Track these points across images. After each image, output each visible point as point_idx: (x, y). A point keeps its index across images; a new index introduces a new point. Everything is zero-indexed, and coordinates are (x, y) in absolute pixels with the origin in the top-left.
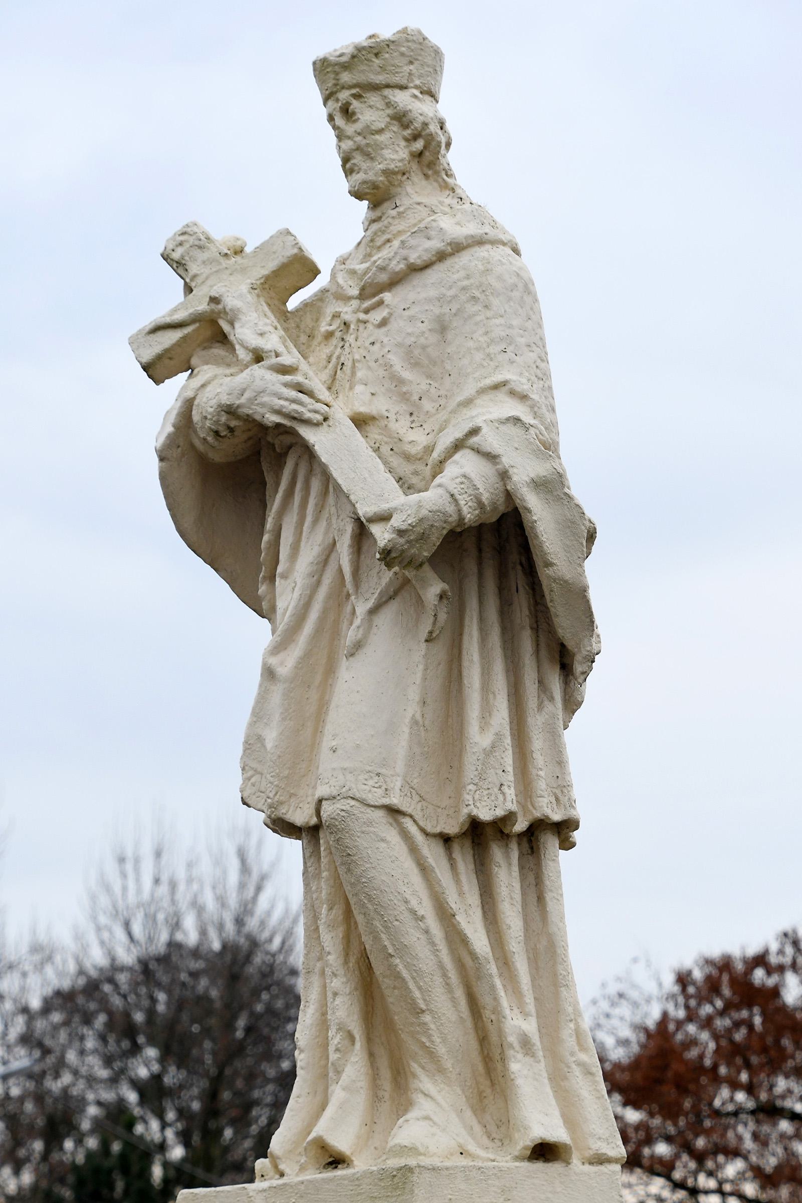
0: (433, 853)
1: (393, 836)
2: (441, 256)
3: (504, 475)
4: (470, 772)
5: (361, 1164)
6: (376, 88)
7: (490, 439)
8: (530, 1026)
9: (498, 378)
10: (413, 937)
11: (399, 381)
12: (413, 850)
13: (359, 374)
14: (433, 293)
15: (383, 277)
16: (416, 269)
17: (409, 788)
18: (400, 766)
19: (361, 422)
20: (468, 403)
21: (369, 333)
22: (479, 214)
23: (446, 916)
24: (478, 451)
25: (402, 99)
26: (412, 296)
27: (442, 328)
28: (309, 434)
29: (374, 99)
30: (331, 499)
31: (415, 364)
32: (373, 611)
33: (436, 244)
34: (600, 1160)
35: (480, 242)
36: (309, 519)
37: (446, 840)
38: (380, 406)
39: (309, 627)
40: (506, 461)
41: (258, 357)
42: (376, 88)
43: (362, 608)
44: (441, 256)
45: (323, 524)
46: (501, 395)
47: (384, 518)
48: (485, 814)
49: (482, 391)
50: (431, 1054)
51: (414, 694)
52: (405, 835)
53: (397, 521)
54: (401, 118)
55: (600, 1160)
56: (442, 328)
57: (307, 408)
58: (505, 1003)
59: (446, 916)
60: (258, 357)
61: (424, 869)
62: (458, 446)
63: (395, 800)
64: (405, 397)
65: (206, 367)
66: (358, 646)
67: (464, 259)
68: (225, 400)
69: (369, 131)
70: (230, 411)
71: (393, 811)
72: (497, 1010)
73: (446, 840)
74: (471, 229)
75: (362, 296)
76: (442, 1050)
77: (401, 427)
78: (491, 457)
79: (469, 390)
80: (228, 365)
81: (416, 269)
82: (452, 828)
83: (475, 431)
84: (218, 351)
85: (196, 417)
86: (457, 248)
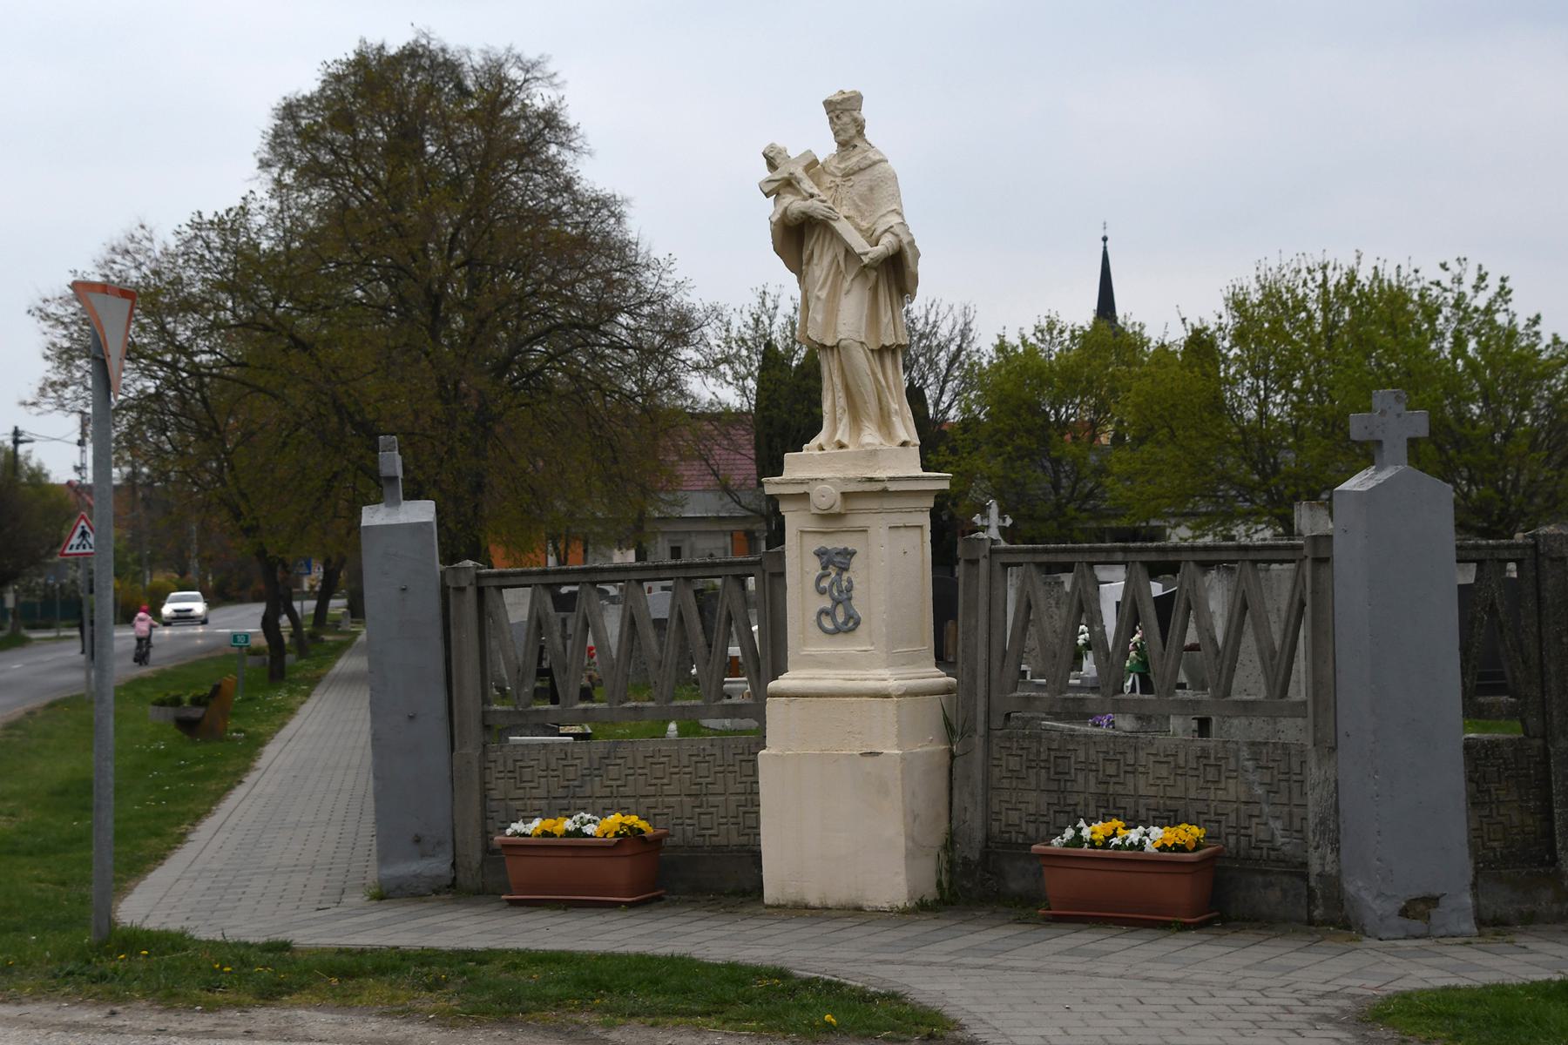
0: (870, 354)
1: (861, 350)
2: (870, 166)
3: (900, 241)
4: (883, 331)
5: (851, 448)
6: (847, 110)
7: (897, 229)
8: (897, 407)
9: (893, 208)
10: (866, 381)
11: (857, 206)
12: (866, 355)
13: (844, 202)
14: (868, 178)
15: (851, 172)
16: (861, 170)
17: (866, 337)
18: (864, 329)
19: (846, 217)
20: (884, 215)
21: (845, 189)
22: (878, 152)
23: (874, 374)
24: (893, 233)
25: (855, 113)
26: (860, 178)
27: (871, 189)
28: (832, 223)
29: (847, 114)
30: (835, 240)
31: (862, 200)
32: (853, 280)
33: (868, 162)
34: (915, 445)
35: (881, 161)
36: (826, 249)
37: (872, 351)
38: (851, 213)
39: (829, 283)
40: (901, 236)
41: (812, 196)
42: (847, 110)
43: (849, 279)
44: (870, 166)
45: (831, 250)
46: (894, 214)
47: (866, 254)
48: (887, 344)
49: (888, 212)
50: (868, 415)
51: (866, 306)
52: (864, 351)
53: (870, 255)
54: (855, 120)
55: (915, 445)
56: (871, 189)
57: (832, 215)
58: (890, 400)
59: (874, 374)
60: (812, 196)
61: (868, 359)
62: (886, 231)
63: (863, 340)
64: (859, 211)
65: (789, 195)
66: (848, 292)
67: (877, 167)
68: (803, 209)
69: (846, 124)
70: (804, 213)
71: (862, 343)
72: (888, 402)
73: (872, 351)
74: (877, 157)
75: (843, 176)
76: (872, 414)
77: (858, 220)
78: (897, 235)
79: (884, 211)
80: (796, 195)
81: (861, 170)
82: (875, 347)
83: (892, 227)
84: (789, 189)
85: (788, 213)
86: (875, 163)
